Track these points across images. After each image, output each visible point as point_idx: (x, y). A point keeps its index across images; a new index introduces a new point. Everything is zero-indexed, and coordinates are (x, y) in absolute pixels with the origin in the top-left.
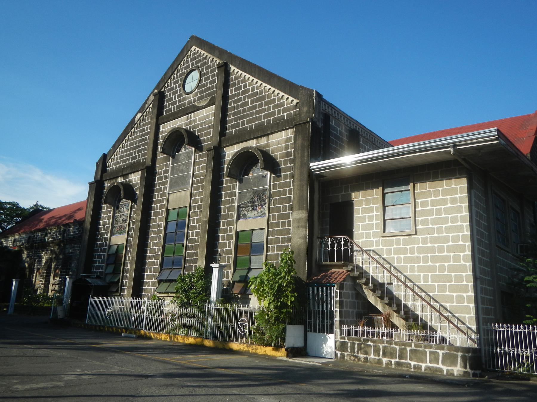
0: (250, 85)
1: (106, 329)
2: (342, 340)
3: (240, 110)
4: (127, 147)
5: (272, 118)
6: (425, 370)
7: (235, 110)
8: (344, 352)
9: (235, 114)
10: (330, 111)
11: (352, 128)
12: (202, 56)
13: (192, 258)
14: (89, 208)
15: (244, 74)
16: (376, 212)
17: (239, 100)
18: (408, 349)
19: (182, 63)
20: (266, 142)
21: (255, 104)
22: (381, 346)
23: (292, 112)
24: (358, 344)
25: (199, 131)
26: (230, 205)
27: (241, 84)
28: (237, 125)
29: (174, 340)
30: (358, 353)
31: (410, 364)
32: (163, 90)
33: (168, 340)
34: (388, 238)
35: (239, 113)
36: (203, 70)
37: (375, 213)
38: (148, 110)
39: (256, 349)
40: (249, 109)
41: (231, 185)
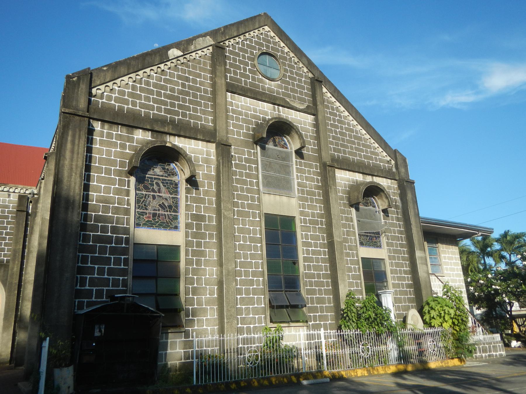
1: (256, 384)
13: (313, 280)
14: (72, 159)
15: (338, 104)
18: (491, 345)
22: (481, 346)
26: (348, 229)
33: (366, 374)
38: (193, 54)
39: (448, 363)
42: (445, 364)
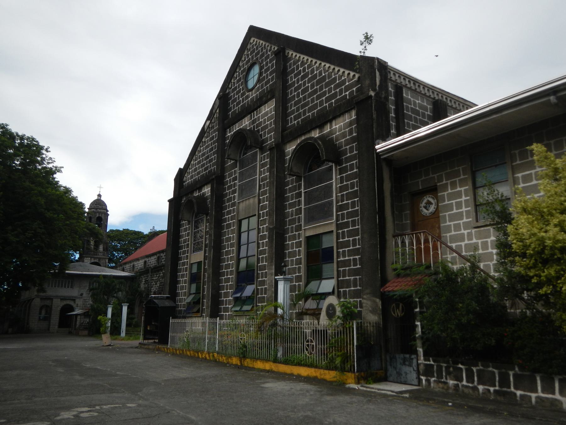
0: (309, 66)
2: (426, 363)
3: (301, 98)
4: (199, 158)
5: (333, 101)
6: (536, 402)
7: (296, 99)
8: (429, 378)
9: (296, 104)
10: (402, 80)
11: (437, 98)
12: (261, 46)
13: (264, 271)
16: (466, 196)
17: (299, 87)
18: (511, 373)
19: (243, 59)
20: (329, 130)
21: (315, 88)
23: (354, 89)
24: (446, 367)
25: (263, 129)
27: (300, 69)
28: (299, 116)
29: (244, 364)
30: (446, 379)
31: (515, 394)
32: (227, 91)
34: (482, 229)
35: (300, 101)
36: (262, 61)
37: (464, 198)
38: (215, 116)
40: (310, 95)
41: (296, 185)
42: (321, 375)
